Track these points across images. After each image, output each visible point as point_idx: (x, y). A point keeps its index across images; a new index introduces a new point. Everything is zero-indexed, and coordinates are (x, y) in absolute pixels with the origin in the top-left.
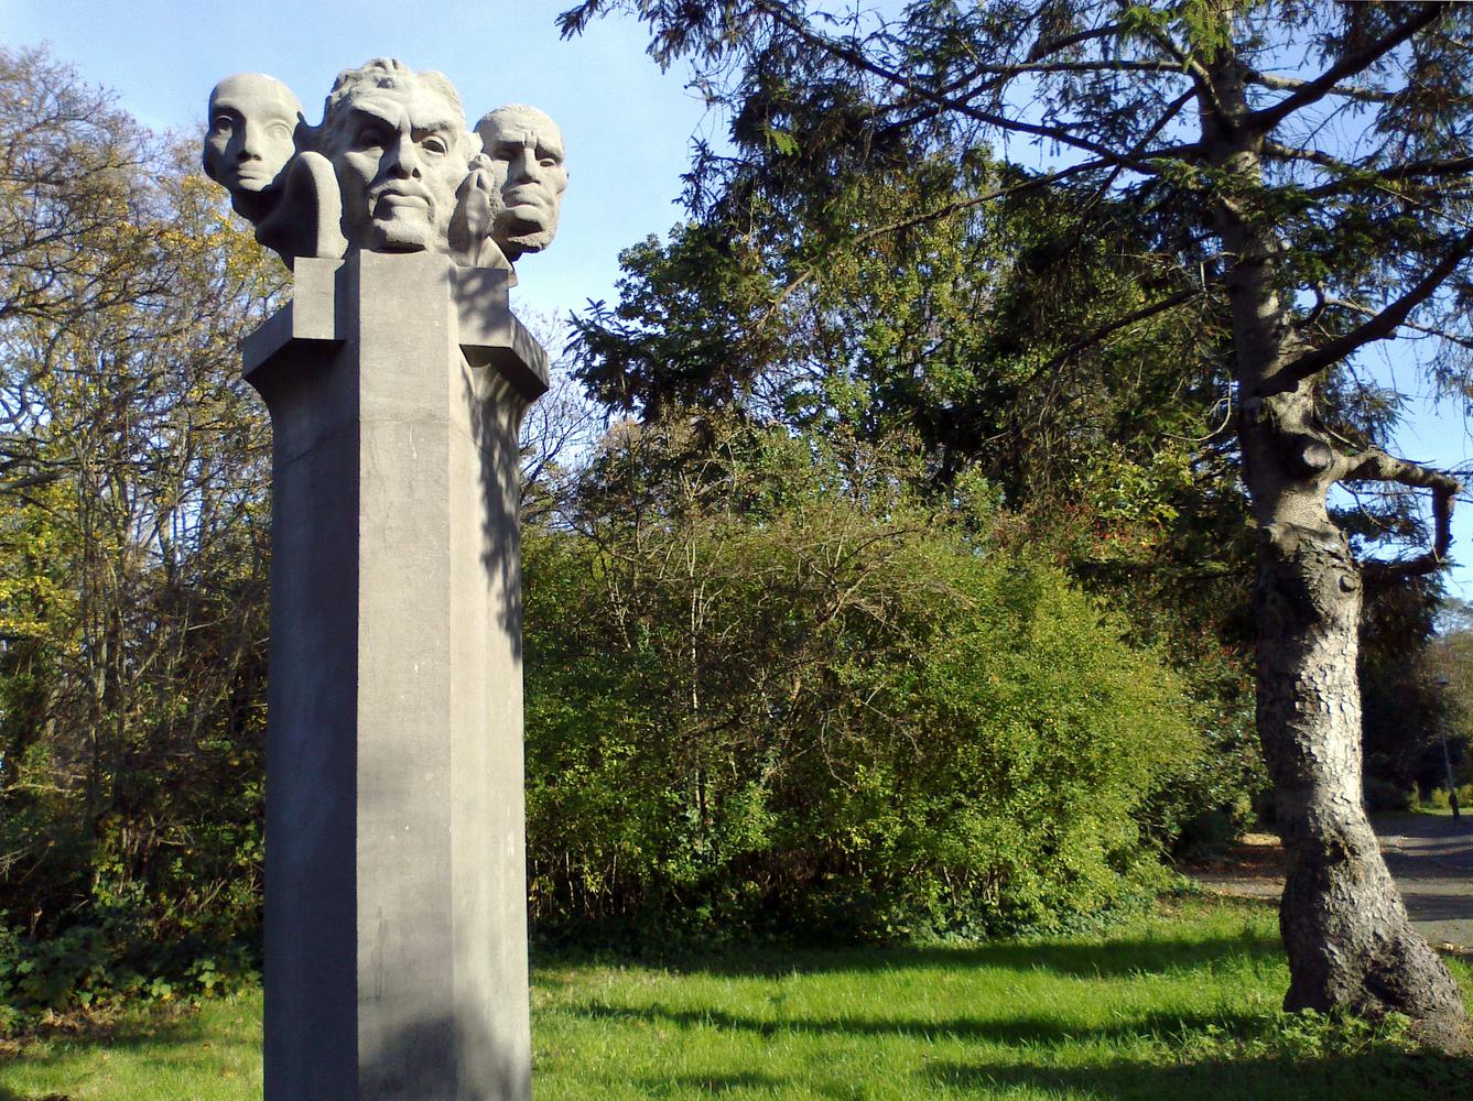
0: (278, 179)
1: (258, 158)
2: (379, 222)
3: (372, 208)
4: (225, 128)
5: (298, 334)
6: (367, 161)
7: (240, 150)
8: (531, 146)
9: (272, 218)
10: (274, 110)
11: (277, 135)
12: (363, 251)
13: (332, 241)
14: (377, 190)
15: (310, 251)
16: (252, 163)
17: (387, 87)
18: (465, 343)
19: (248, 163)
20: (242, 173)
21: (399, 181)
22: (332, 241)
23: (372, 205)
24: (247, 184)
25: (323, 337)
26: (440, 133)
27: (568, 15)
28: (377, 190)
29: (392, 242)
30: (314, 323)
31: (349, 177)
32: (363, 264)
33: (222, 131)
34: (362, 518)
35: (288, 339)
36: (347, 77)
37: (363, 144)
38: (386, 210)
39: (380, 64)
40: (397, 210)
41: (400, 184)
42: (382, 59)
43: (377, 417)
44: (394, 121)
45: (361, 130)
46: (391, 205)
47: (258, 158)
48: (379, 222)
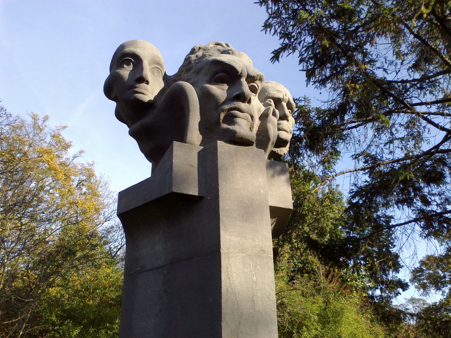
0: (156, 97)
1: (147, 83)
2: (225, 126)
4: (128, 65)
6: (220, 91)
7: (138, 76)
8: (285, 102)
9: (148, 120)
10: (157, 60)
11: (156, 74)
12: (219, 142)
13: (194, 135)
14: (227, 107)
15: (182, 138)
16: (144, 85)
17: (229, 53)
18: (273, 205)
19: (142, 84)
20: (137, 90)
21: (240, 103)
22: (194, 135)
23: (222, 116)
25: (190, 193)
26: (258, 82)
27: (276, 51)
28: (227, 107)
29: (238, 138)
31: (206, 98)
32: (219, 149)
33: (125, 66)
34: (223, 324)
35: (167, 192)
36: (200, 48)
37: (218, 81)
38: (231, 119)
39: (218, 44)
40: (238, 120)
41: (243, 105)
42: (219, 42)
43: (231, 250)
44: (239, 69)
45: (217, 73)
46: (236, 117)
47: (147, 83)
48: (225, 126)
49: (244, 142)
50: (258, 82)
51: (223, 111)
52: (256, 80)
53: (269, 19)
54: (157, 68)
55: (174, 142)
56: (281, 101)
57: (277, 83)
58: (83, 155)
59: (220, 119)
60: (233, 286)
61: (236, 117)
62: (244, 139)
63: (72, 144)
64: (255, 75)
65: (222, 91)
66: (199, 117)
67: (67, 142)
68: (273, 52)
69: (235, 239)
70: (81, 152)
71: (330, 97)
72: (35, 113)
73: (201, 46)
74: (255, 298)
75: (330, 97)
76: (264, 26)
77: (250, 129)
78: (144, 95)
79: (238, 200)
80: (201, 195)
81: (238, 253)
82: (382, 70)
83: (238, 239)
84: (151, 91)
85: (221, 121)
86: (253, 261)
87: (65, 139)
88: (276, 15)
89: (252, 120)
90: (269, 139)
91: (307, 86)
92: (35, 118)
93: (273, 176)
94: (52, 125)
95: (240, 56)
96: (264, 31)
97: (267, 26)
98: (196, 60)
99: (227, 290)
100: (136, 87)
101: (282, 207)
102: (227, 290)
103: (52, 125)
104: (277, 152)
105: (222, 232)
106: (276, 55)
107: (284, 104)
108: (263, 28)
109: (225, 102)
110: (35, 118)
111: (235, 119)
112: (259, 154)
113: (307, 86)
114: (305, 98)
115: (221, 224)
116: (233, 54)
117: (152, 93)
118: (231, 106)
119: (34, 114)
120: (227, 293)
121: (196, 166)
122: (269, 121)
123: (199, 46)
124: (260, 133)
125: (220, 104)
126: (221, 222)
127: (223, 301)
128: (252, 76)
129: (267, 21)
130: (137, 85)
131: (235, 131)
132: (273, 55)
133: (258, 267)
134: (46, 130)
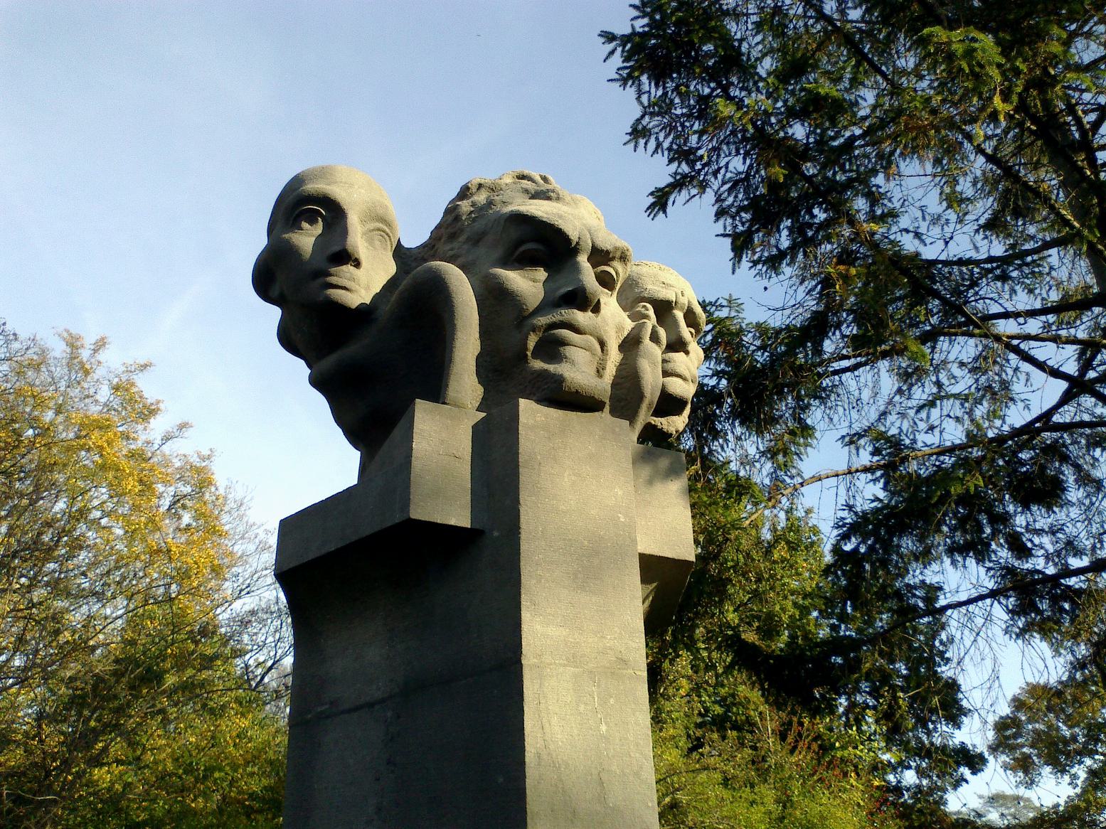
0: (377, 297)
1: (357, 264)
2: (538, 364)
3: (531, 344)
4: (312, 222)
5: (420, 512)
6: (528, 284)
7: (336, 248)
8: (681, 309)
9: (353, 350)
10: (381, 212)
11: (377, 243)
12: (522, 402)
13: (466, 384)
14: (543, 320)
15: (436, 391)
16: (348, 269)
17: (549, 198)
18: (647, 552)
19: (344, 268)
20: (333, 280)
21: (575, 311)
22: (466, 384)
23: (532, 341)
24: (336, 294)
25: (453, 522)
26: (616, 264)
27: (659, 190)
28: (543, 320)
30: (444, 497)
31: (495, 300)
32: (523, 419)
33: (305, 225)
35: (398, 518)
36: (480, 186)
37: (523, 261)
38: (552, 348)
39: (522, 177)
40: (569, 351)
41: (581, 317)
42: (526, 172)
44: (574, 236)
45: (521, 242)
46: (564, 343)
47: (357, 264)
48: (538, 364)
49: (580, 402)
50: (616, 264)
51: (534, 331)
52: (613, 259)
53: (643, 117)
54: (379, 230)
55: (418, 401)
56: (672, 308)
57: (663, 267)
58: (186, 434)
59: (527, 349)
60: (552, 747)
61: (564, 343)
62: (582, 395)
63: (162, 406)
64: (609, 248)
65: (531, 283)
66: (478, 343)
67: (149, 401)
68: (652, 194)
69: (555, 632)
70: (183, 426)
71: (788, 297)
72: (73, 332)
73: (483, 181)
74: (605, 777)
75: (788, 297)
76: (630, 134)
77: (598, 371)
78: (348, 293)
79: (564, 540)
80: (478, 527)
81: (565, 665)
82: (911, 235)
83: (564, 632)
84: (366, 281)
85: (529, 354)
86: (599, 686)
87: (146, 395)
88: (660, 107)
89: (602, 350)
90: (640, 396)
91: (733, 272)
92: (73, 343)
93: (650, 482)
94: (113, 361)
95: (576, 204)
96: (632, 145)
97: (638, 133)
98: (472, 212)
99: (539, 756)
100: (331, 275)
101: (670, 556)
102: (539, 756)
103: (113, 361)
104: (660, 427)
105: (526, 615)
106: (660, 201)
107: (679, 315)
108: (628, 137)
109: (539, 310)
110: (73, 343)
111: (561, 349)
112: (617, 430)
113: (733, 272)
114: (730, 301)
115: (523, 596)
116: (558, 199)
117: (368, 288)
118: (554, 319)
119: (70, 335)
120: (539, 765)
121: (468, 458)
122: (642, 353)
123: (477, 181)
124: (619, 381)
125: (526, 314)
126: (523, 591)
127: (529, 782)
128: (602, 251)
129: (639, 121)
130: (333, 270)
131: (561, 376)
132: (651, 200)
133: (612, 701)
134: (99, 373)
